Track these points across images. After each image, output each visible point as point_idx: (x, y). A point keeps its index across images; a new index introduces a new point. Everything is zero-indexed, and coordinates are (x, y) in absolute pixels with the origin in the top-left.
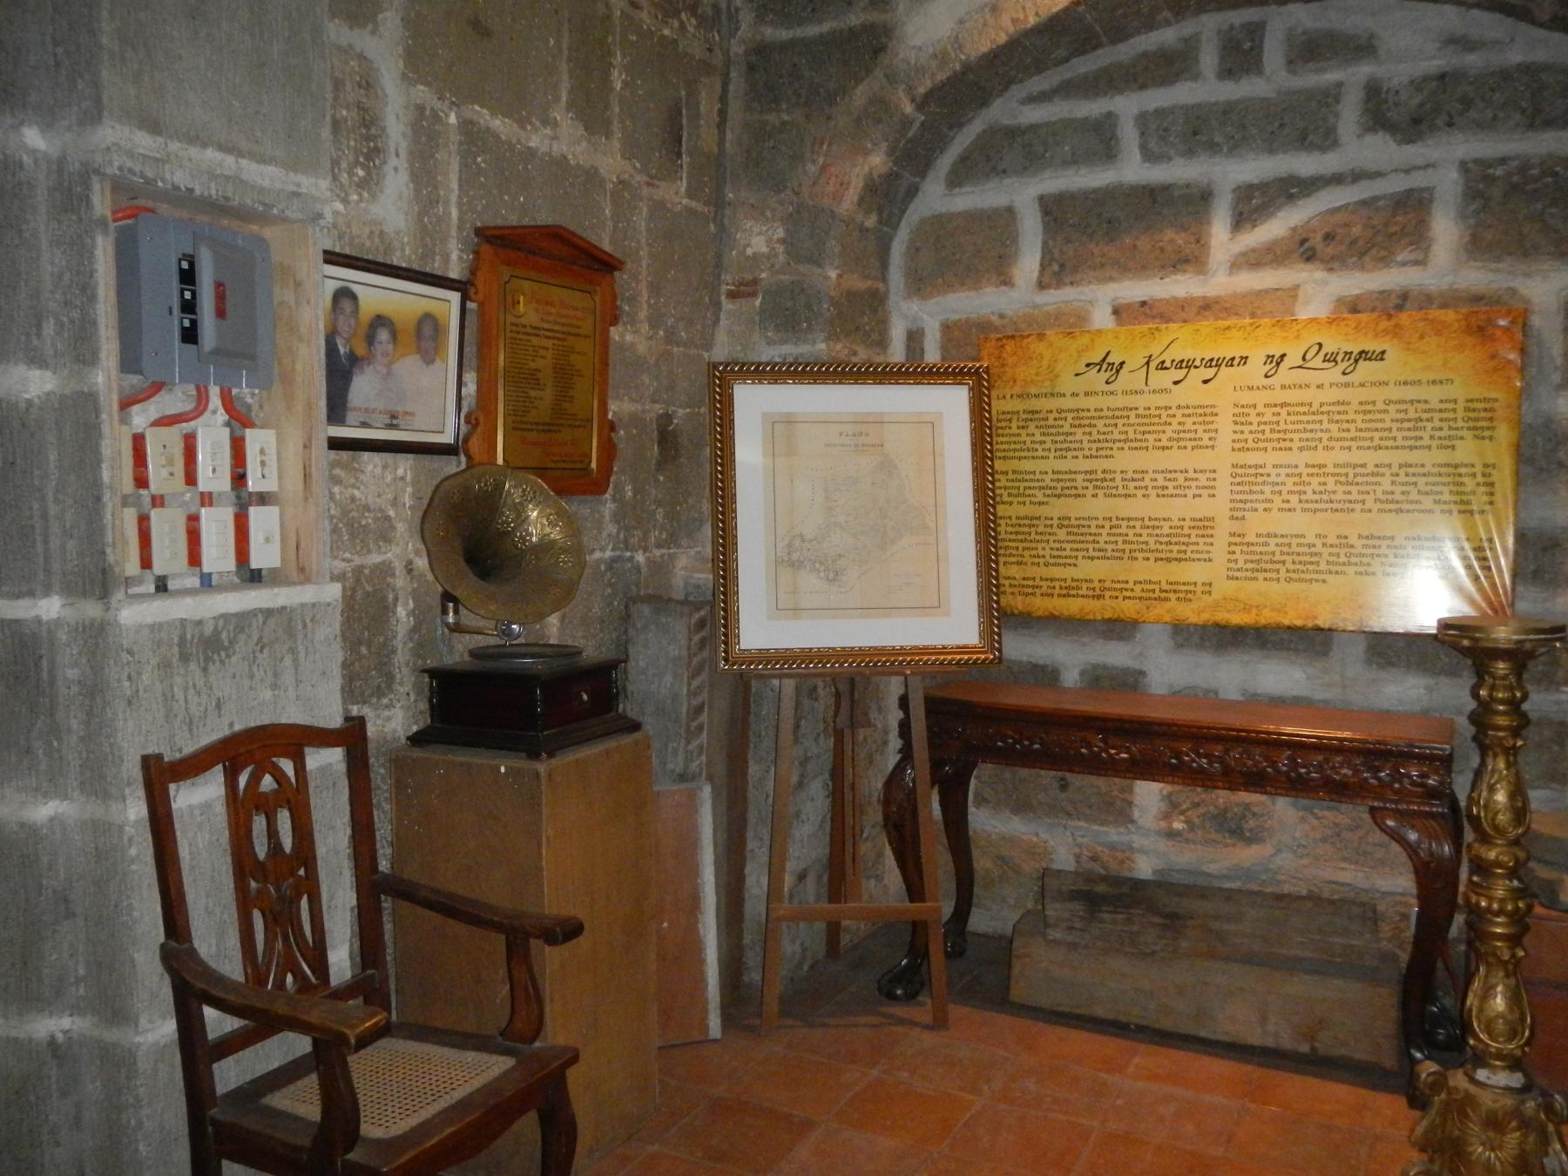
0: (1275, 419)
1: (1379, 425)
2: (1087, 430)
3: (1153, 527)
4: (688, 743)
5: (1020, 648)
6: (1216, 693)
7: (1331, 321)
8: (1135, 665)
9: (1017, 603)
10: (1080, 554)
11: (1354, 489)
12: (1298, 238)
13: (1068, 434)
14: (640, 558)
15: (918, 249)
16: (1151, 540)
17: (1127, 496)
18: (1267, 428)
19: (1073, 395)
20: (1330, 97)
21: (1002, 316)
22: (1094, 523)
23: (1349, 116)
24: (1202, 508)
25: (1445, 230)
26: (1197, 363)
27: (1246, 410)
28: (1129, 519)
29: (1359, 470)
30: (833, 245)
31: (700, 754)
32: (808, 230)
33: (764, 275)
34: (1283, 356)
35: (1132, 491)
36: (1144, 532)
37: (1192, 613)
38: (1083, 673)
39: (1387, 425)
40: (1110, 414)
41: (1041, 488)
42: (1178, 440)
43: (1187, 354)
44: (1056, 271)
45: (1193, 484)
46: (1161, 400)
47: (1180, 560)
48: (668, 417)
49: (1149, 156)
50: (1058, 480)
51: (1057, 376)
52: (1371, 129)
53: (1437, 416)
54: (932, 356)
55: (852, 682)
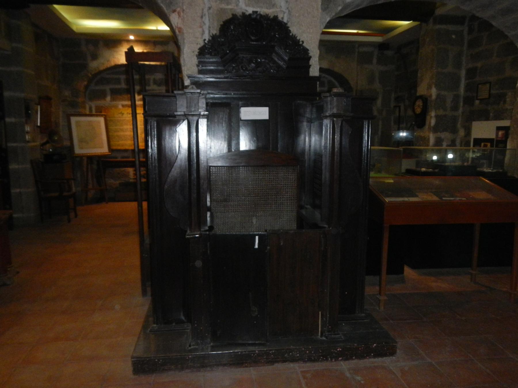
44: (113, 99)
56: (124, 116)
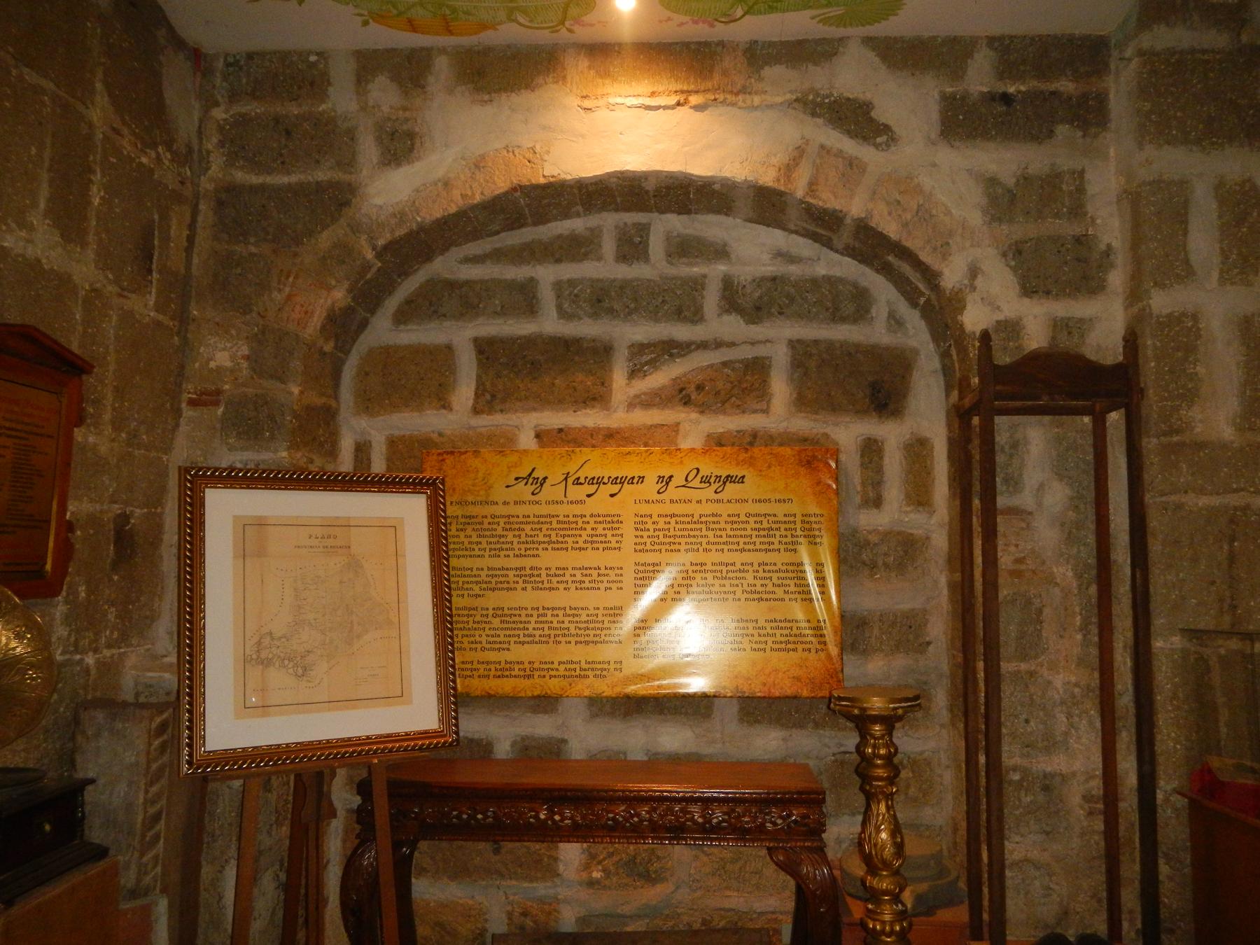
0: (666, 527)
1: (743, 533)
2: (517, 533)
3: (574, 615)
4: (142, 855)
5: (473, 725)
6: (625, 754)
7: (705, 452)
8: (558, 735)
9: (477, 685)
10: (512, 640)
11: (727, 582)
12: (677, 387)
13: (500, 536)
14: (90, 660)
15: (367, 374)
16: (572, 626)
17: (551, 589)
18: (661, 534)
19: (505, 503)
20: (697, 285)
21: (440, 435)
22: (523, 613)
23: (711, 300)
24: (611, 599)
25: (780, 388)
26: (606, 480)
27: (644, 519)
28: (553, 609)
29: (730, 568)
30: (296, 364)
31: (155, 866)
32: (270, 351)
33: (227, 387)
34: (671, 477)
35: (555, 585)
36: (567, 619)
37: (605, 688)
38: (514, 744)
39: (749, 532)
40: (536, 520)
41: (477, 583)
42: (592, 542)
43: (597, 473)
44: (487, 400)
45: (605, 579)
46: (577, 509)
47: (596, 643)
48: (124, 518)
49: (563, 314)
50: (492, 576)
51: (490, 487)
52: (728, 311)
53: (783, 526)
54: (378, 466)
55: (320, 775)
56: (547, 492)
